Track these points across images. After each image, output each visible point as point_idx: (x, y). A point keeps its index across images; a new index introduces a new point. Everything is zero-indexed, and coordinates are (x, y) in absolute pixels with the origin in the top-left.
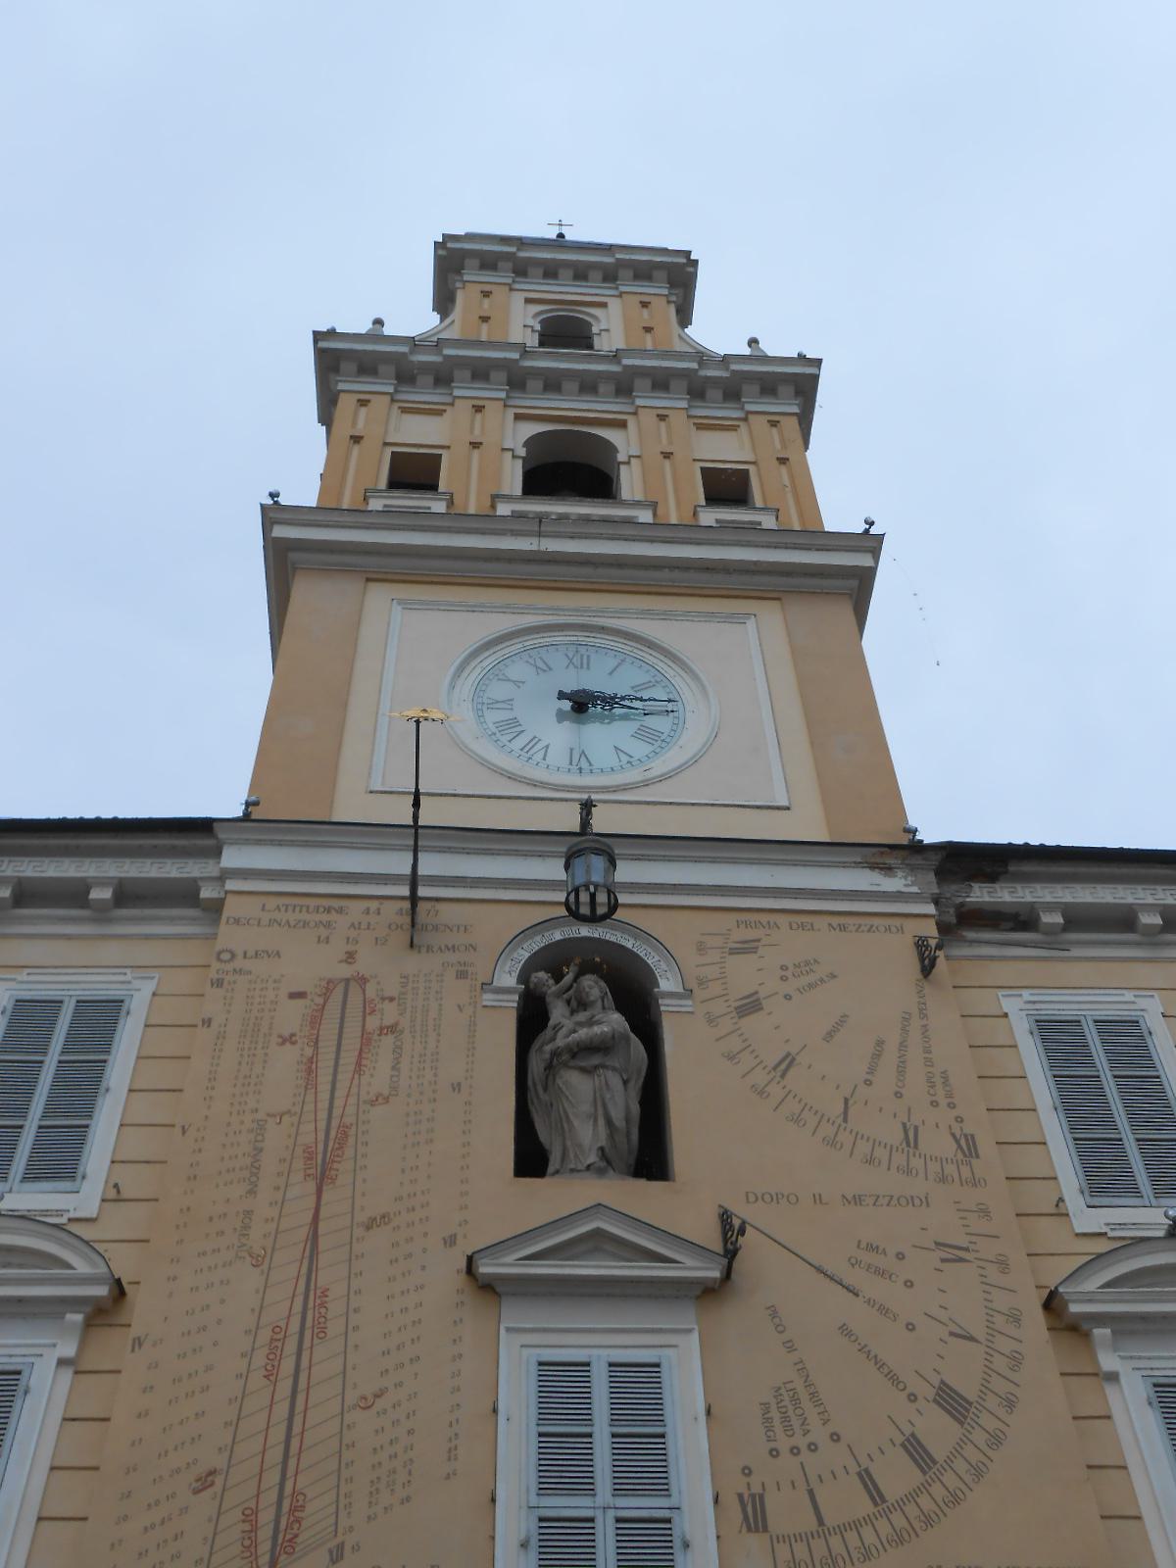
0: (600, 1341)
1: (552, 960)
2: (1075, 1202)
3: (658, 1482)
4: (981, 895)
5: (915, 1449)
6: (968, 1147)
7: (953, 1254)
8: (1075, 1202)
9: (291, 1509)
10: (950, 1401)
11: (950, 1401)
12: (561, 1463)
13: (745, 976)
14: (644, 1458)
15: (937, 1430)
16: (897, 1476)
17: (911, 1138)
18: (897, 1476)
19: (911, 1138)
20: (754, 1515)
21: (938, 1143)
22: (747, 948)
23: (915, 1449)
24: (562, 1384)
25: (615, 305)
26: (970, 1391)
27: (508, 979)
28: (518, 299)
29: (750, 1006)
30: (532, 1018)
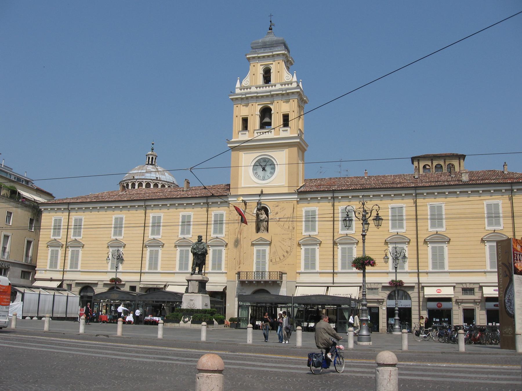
0: (261, 248)
3: (265, 258)
5: (284, 256)
9: (240, 261)
10: (287, 252)
11: (287, 252)
13: (277, 209)
14: (264, 256)
15: (285, 254)
18: (282, 258)
20: (271, 261)
21: (291, 228)
22: (277, 206)
23: (284, 256)
24: (258, 251)
25: (274, 63)
26: (288, 251)
27: (255, 212)
28: (259, 64)
29: (277, 213)
30: (258, 215)
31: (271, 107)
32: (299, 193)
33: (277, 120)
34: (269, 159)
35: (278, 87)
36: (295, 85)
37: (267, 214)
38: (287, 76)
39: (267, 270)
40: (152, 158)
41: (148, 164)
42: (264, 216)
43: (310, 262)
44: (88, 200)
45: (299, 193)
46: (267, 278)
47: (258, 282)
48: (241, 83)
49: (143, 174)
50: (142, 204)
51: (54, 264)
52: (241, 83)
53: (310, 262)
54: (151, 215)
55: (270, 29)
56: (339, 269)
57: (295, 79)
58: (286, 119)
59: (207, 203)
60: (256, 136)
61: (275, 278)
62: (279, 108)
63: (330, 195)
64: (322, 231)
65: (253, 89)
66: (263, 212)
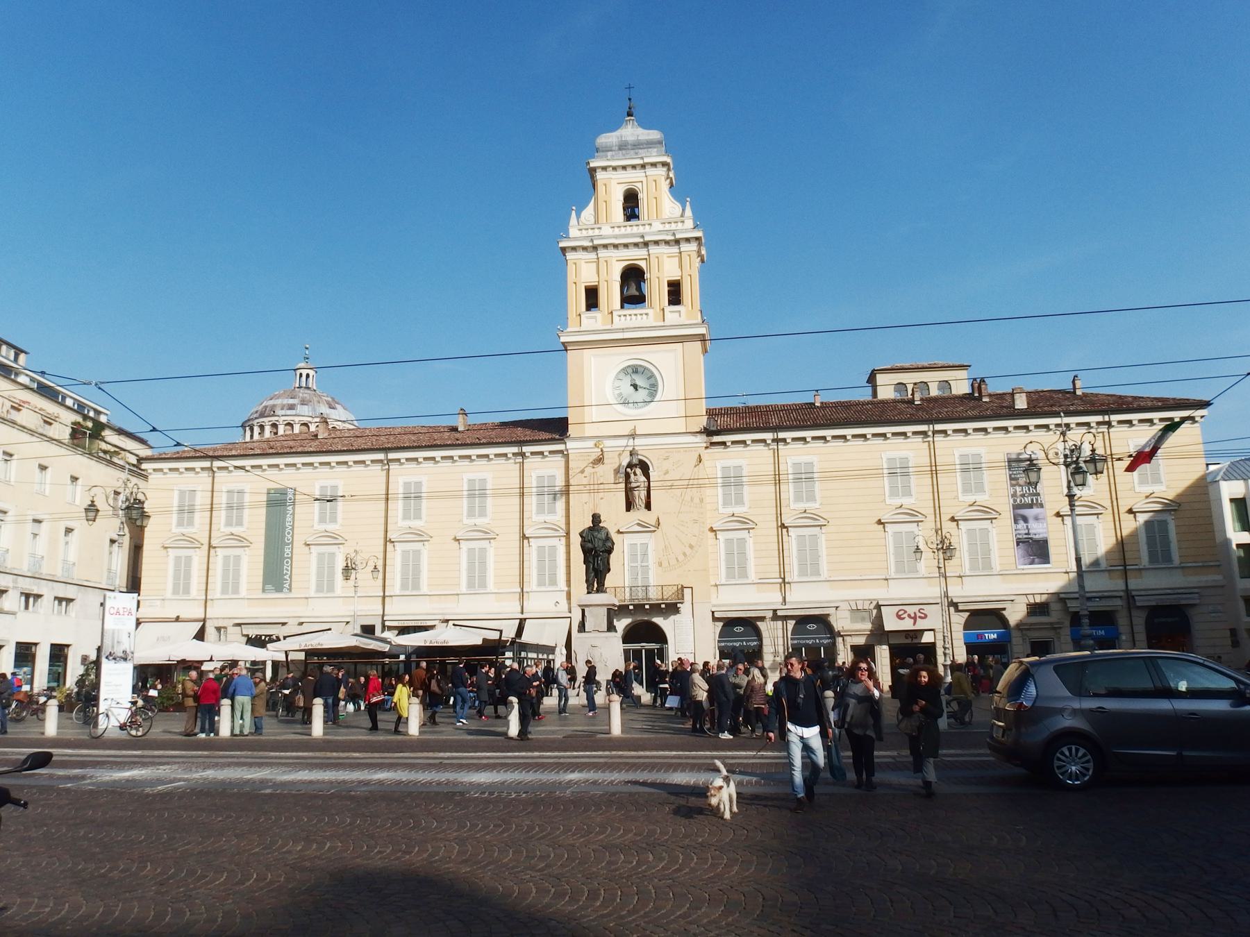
1: (630, 465)
2: (720, 507)
4: (716, 439)
5: (685, 554)
6: (702, 500)
7: (696, 521)
8: (720, 507)
10: (691, 547)
11: (691, 547)
12: (633, 557)
15: (688, 551)
16: (681, 558)
17: (692, 499)
18: (681, 558)
19: (692, 499)
20: (660, 564)
21: (697, 500)
22: (667, 458)
23: (685, 554)
31: (643, 264)
32: (708, 432)
33: (656, 290)
34: (645, 368)
35: (657, 226)
36: (689, 224)
37: (647, 474)
38: (670, 207)
39: (652, 582)
40: (308, 376)
41: (300, 387)
42: (643, 479)
43: (737, 568)
44: (259, 452)
45: (708, 432)
46: (654, 595)
47: (639, 608)
48: (578, 216)
49: (292, 407)
50: (381, 456)
51: (181, 586)
52: (578, 216)
53: (737, 568)
54: (401, 480)
55: (630, 114)
56: (793, 575)
57: (688, 212)
58: (675, 293)
59: (523, 455)
60: (619, 322)
61: (669, 595)
62: (663, 268)
63: (768, 436)
64: (757, 501)
65: (607, 230)
66: (638, 471)
